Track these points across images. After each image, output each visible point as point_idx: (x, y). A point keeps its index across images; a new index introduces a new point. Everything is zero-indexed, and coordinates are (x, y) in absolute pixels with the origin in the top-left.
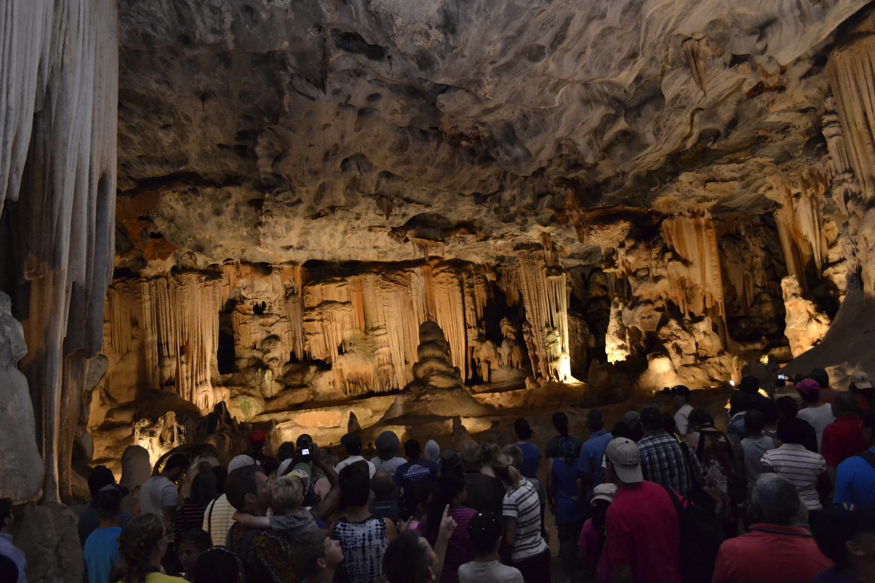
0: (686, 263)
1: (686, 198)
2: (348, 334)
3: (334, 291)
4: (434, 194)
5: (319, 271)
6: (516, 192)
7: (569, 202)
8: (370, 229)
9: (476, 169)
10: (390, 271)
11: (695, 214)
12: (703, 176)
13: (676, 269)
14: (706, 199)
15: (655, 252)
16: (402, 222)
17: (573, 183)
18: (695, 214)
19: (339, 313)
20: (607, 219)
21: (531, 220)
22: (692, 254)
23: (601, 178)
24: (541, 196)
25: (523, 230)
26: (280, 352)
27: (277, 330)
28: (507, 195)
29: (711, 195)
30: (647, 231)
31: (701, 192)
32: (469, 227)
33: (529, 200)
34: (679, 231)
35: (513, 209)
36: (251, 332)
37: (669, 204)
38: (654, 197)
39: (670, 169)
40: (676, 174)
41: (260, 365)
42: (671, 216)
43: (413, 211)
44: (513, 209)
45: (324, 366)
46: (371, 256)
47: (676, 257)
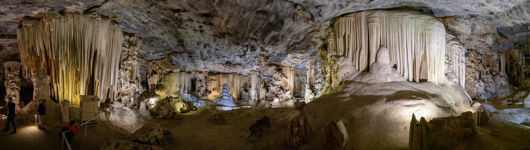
0: (287, 78)
1: (289, 62)
2: (215, 86)
3: (213, 77)
4: (230, 55)
5: (211, 73)
6: (249, 56)
7: (262, 60)
8: (218, 64)
9: (236, 46)
10: (225, 74)
11: (290, 67)
12: (293, 56)
13: (284, 78)
14: (293, 64)
15: (280, 74)
16: (225, 62)
17: (263, 55)
18: (290, 67)
19: (214, 82)
20: (271, 65)
21: (254, 64)
22: (288, 76)
23: (269, 53)
24: (255, 57)
25: (252, 66)
26: (203, 89)
27: (203, 85)
28: (247, 56)
29: (294, 62)
30: (279, 69)
31: (292, 61)
32: (240, 65)
33: (253, 59)
34: (286, 70)
35: (249, 60)
36: (198, 85)
37: (285, 63)
38: (281, 61)
39: (286, 53)
40: (287, 54)
41: (199, 91)
42: (285, 67)
43: (226, 60)
44: (249, 60)
45: (210, 92)
46: (222, 71)
47: (285, 76)
